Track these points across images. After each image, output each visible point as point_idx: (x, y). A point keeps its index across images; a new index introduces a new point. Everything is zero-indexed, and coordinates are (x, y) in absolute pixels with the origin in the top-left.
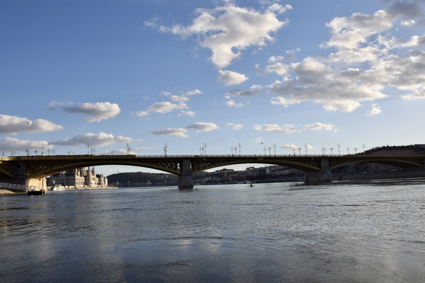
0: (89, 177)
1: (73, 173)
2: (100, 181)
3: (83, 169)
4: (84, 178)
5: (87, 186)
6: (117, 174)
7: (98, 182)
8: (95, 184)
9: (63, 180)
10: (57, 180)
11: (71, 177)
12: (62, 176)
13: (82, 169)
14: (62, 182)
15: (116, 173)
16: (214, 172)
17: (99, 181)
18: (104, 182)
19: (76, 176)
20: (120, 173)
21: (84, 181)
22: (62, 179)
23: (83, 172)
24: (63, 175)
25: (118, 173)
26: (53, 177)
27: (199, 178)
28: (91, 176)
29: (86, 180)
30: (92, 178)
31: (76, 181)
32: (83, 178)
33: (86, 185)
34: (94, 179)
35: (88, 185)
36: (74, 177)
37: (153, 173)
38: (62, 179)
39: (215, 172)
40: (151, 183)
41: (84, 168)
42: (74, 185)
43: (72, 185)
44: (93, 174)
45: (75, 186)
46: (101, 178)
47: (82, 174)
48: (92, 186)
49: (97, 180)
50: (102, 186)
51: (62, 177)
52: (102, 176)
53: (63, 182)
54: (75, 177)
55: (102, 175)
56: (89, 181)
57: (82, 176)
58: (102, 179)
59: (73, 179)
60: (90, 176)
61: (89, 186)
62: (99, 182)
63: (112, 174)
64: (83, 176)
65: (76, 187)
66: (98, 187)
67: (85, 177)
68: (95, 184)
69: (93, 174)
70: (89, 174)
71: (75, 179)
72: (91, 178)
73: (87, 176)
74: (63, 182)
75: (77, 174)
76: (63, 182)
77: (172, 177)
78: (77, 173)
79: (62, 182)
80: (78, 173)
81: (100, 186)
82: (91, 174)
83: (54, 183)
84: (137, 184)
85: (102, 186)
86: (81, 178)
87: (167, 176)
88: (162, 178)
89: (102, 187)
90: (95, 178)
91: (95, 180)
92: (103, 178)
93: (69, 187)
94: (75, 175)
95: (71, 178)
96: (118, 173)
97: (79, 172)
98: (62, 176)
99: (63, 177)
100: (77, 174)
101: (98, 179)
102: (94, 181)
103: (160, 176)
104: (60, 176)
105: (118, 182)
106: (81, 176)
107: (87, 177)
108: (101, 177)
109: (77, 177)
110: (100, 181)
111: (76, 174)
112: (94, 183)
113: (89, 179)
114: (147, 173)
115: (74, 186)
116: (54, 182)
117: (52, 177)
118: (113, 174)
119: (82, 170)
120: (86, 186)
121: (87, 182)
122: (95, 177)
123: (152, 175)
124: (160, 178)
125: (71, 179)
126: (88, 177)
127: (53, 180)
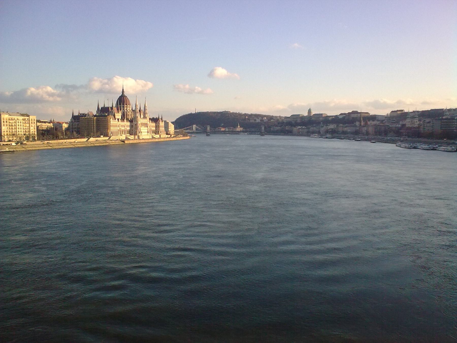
0: (136, 121)
2: (157, 127)
3: (128, 108)
4: (129, 124)
5: (133, 136)
6: (194, 114)
7: (154, 129)
8: (148, 133)
13: (125, 108)
16: (336, 116)
17: (156, 127)
18: (164, 128)
19: (111, 120)
20: (198, 112)
21: (129, 128)
25: (196, 112)
27: (314, 125)
28: (141, 121)
29: (131, 126)
31: (112, 129)
32: (127, 124)
33: (132, 135)
34: (146, 125)
35: (135, 134)
37: (245, 113)
39: (339, 115)
40: (242, 129)
41: (129, 107)
45: (110, 138)
46: (159, 123)
48: (141, 138)
49: (152, 127)
50: (160, 136)
52: (160, 120)
55: (160, 117)
56: (137, 128)
57: (125, 120)
58: (162, 124)
60: (138, 120)
61: (137, 137)
62: (156, 129)
63: (187, 114)
64: (127, 119)
67: (131, 121)
68: (148, 132)
69: (145, 117)
70: (136, 117)
72: (139, 122)
77: (272, 120)
81: (158, 136)
84: (223, 129)
85: (160, 136)
86: (122, 123)
87: (265, 118)
88: (258, 121)
90: (148, 123)
91: (147, 127)
92: (164, 122)
96: (196, 112)
97: (118, 112)
101: (154, 124)
102: (147, 128)
103: (255, 119)
105: (194, 126)
107: (133, 122)
108: (159, 121)
109: (112, 122)
110: (157, 127)
112: (147, 131)
114: (236, 113)
118: (190, 113)
120: (132, 137)
121: (133, 130)
122: (147, 121)
123: (243, 117)
124: (255, 120)
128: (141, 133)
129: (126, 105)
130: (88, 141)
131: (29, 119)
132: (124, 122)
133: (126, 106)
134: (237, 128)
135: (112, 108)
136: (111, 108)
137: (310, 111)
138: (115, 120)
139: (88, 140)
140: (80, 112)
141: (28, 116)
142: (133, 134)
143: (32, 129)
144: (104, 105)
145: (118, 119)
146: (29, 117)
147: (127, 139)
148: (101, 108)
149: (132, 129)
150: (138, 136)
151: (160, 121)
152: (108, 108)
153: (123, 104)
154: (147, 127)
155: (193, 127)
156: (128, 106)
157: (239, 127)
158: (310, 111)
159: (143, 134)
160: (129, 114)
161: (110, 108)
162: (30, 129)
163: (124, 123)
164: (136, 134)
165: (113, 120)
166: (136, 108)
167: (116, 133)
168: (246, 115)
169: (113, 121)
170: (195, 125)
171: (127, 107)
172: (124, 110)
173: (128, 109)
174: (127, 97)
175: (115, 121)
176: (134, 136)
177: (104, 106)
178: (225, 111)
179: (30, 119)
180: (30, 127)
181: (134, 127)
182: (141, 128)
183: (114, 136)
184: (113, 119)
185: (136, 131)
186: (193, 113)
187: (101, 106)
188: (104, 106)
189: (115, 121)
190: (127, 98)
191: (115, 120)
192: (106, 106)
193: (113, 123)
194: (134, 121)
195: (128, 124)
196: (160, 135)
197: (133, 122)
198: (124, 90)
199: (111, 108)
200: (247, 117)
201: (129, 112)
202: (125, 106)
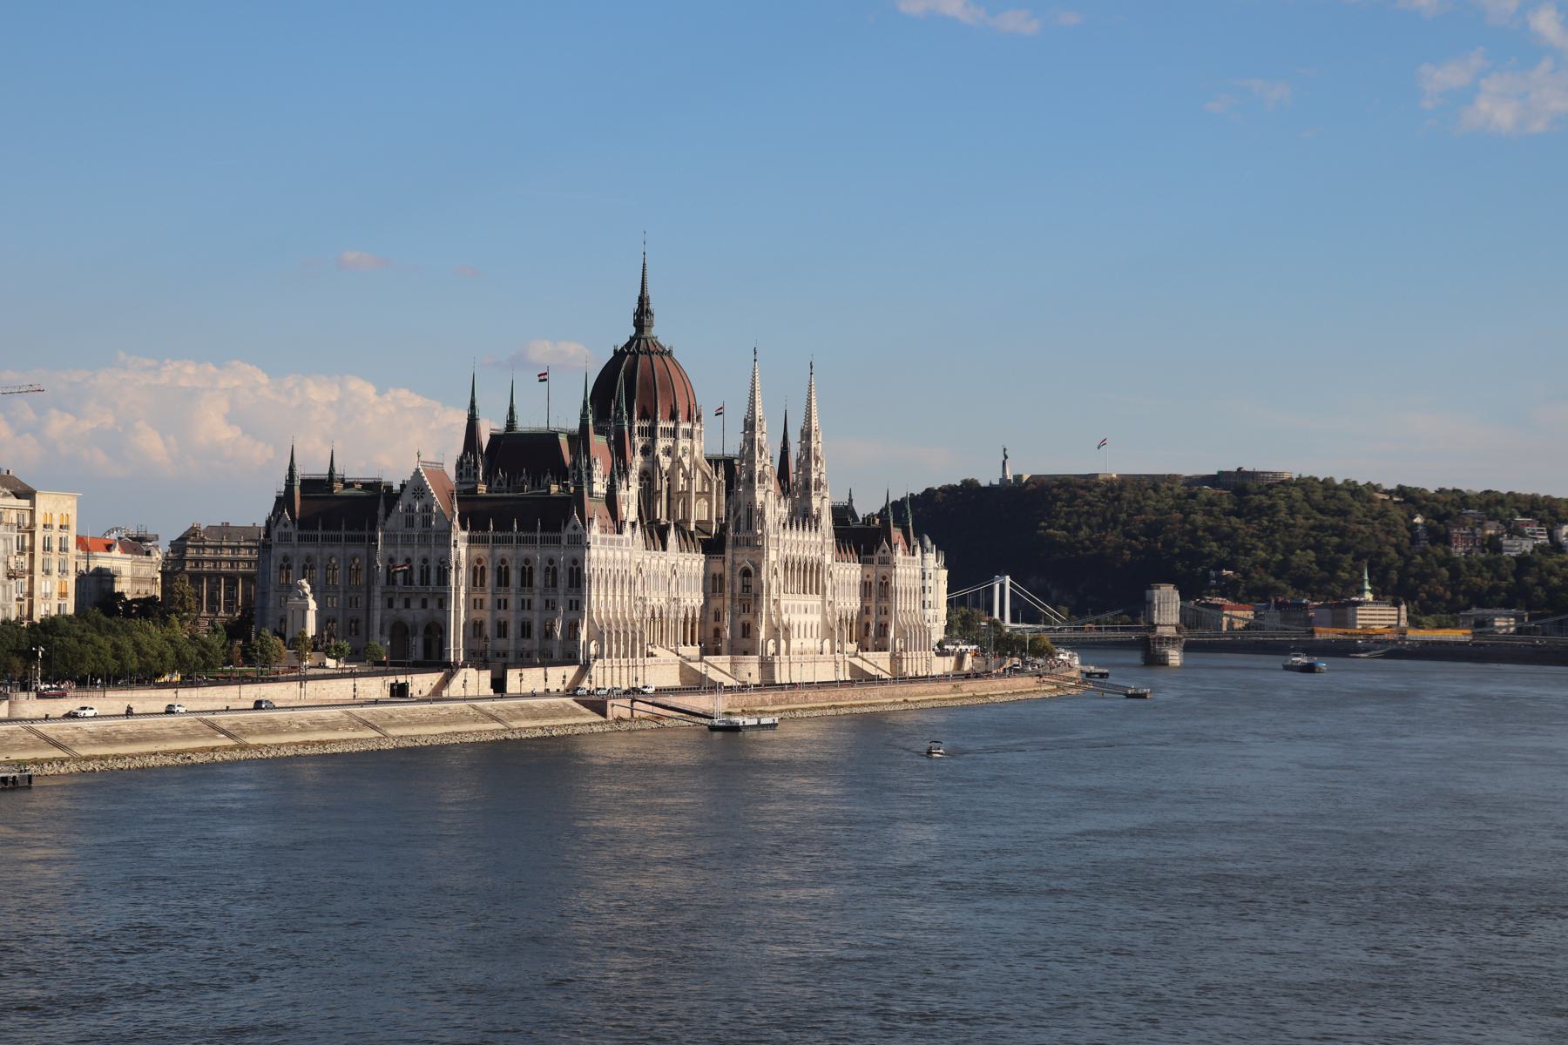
1: (554, 488)
3: (683, 443)
4: (694, 563)
6: (991, 488)
9: (425, 579)
10: (352, 572)
11: (526, 551)
12: (410, 522)
13: (662, 443)
14: (416, 605)
15: (988, 477)
19: (595, 532)
22: (417, 564)
23: (671, 476)
24: (427, 522)
26: (300, 538)
30: (789, 565)
31: (601, 602)
33: (717, 652)
34: (808, 575)
35: (744, 642)
36: (575, 553)
38: (417, 564)
42: (569, 658)
43: (547, 661)
44: (802, 516)
45: (585, 668)
47: (661, 512)
51: (408, 541)
53: (424, 605)
54: (580, 543)
57: (672, 537)
59: (551, 571)
64: (681, 527)
66: (861, 678)
67: (712, 547)
68: (828, 632)
69: (802, 516)
71: (577, 578)
72: (773, 556)
73: (723, 528)
74: (432, 604)
75: (611, 501)
76: (432, 604)
78: (600, 487)
79: (416, 605)
80: (622, 493)
81: (877, 663)
82: (770, 502)
83: (311, 629)
85: (896, 660)
89: (900, 678)
93: (499, 685)
94: (586, 522)
95: (527, 561)
96: (1004, 479)
98: (417, 531)
99: (425, 540)
100: (602, 508)
102: (814, 601)
104: (396, 521)
106: (656, 534)
111: (595, 509)
113: (746, 573)
115: (571, 671)
116: (313, 605)
117: (285, 538)
119: (668, 452)
120: (719, 668)
122: (818, 543)
125: (527, 578)
126: (736, 543)
127: (290, 588)
128: (787, 629)
129: (643, 417)
130: (445, 694)
131: (32, 513)
132: (664, 549)
133: (646, 424)
134: (1359, 603)
135: (579, 440)
136: (571, 438)
138: (616, 537)
139: (445, 682)
140: (336, 465)
141: (27, 494)
142: (724, 646)
143: (47, 596)
145: (633, 525)
146: (33, 504)
147: (696, 683)
148: (492, 436)
149: (716, 603)
150: (767, 666)
151: (900, 548)
152: (550, 438)
153: (648, 414)
154: (819, 589)
155: (991, 589)
156: (688, 426)
157: (1369, 596)
159: (795, 644)
160: (689, 492)
161: (563, 439)
162: (36, 593)
163: (662, 562)
164: (746, 643)
165: (608, 536)
166: (750, 441)
167: (633, 643)
168: (1409, 497)
169: (603, 541)
170: (1008, 579)
171: (673, 433)
172: (650, 458)
173: (659, 451)
174: (669, 353)
175: (620, 542)
176: (732, 663)
178: (1239, 469)
179: (39, 520)
180: (36, 578)
181: (728, 590)
182: (785, 601)
183: (610, 656)
184: (604, 529)
185: (746, 618)
186: (984, 483)
189: (620, 542)
190: (674, 362)
191: (620, 532)
193: (602, 554)
194: (729, 542)
195: (654, 562)
196: (893, 657)
197: (729, 552)
198: (653, 305)
199: (571, 438)
200: (1418, 520)
201: (687, 477)
202: (662, 424)
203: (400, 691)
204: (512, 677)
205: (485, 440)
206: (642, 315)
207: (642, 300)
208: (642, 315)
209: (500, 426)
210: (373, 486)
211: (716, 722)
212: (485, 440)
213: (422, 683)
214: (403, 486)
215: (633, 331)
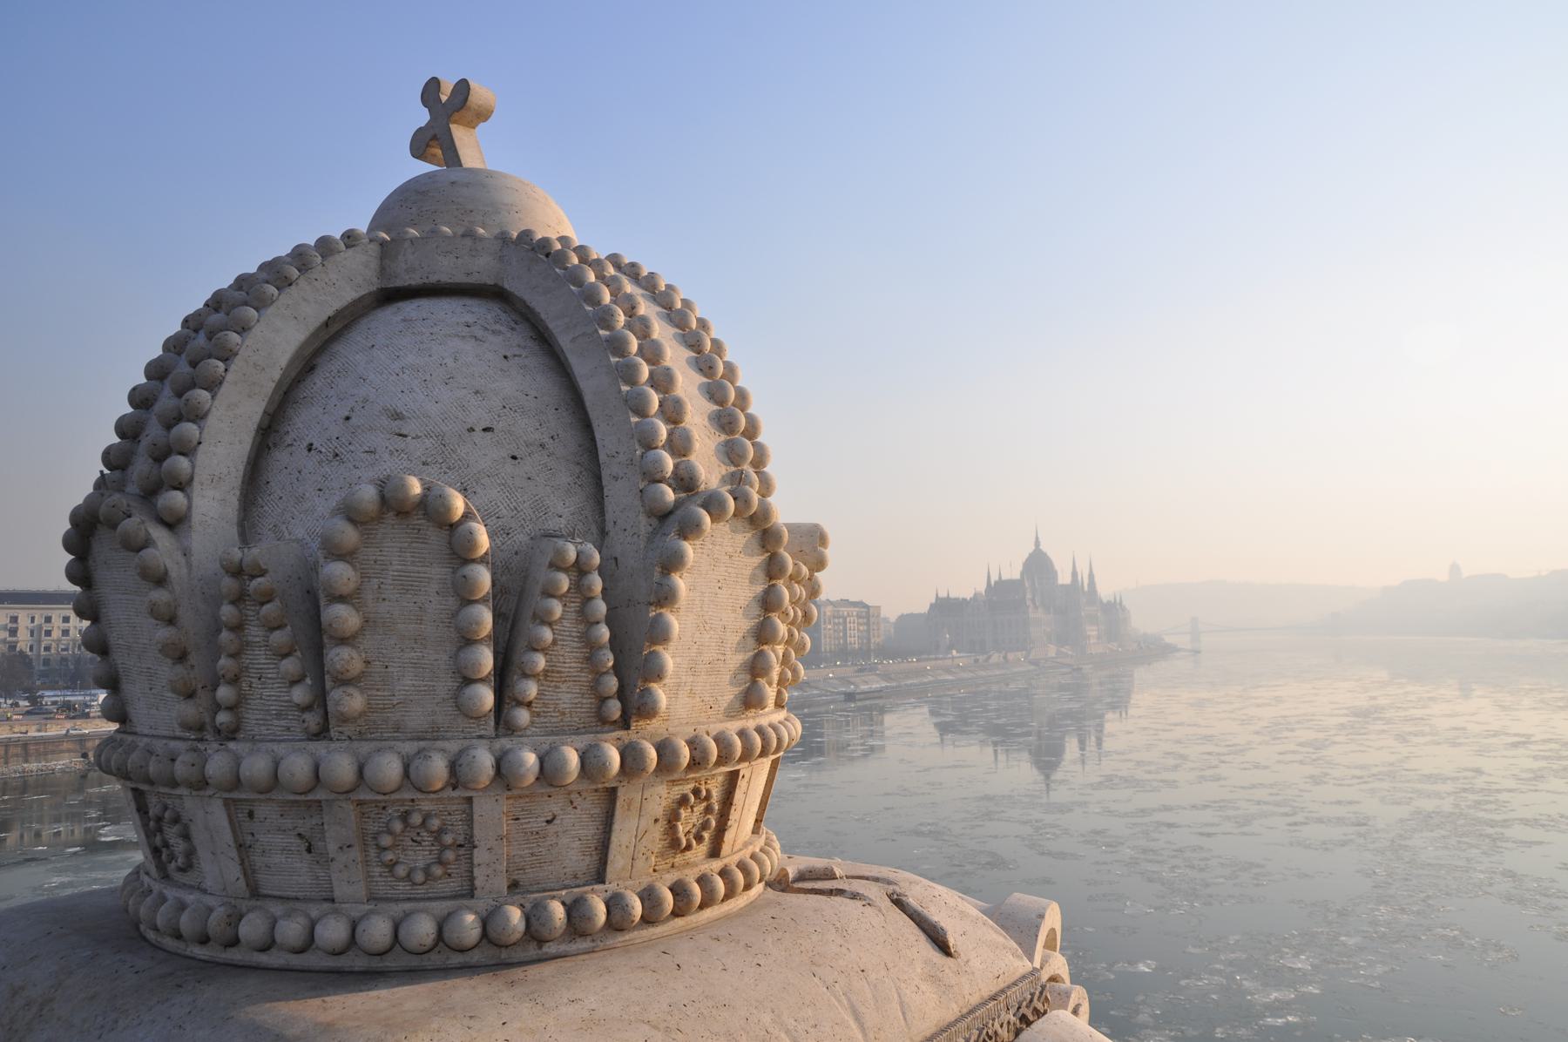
65: (1031, 657)
75: (1033, 600)
94: (1028, 607)
112: (1095, 633)
137: (1455, 569)
144: (1000, 574)
148: (996, 582)
158: (1455, 569)
177: (1000, 577)
187: (994, 578)
188: (1000, 577)
192: (1003, 578)
198: (1040, 540)
203: (976, 661)
204: (1009, 654)
205: (993, 583)
206: (1037, 543)
207: (1037, 538)
208: (1037, 543)
209: (997, 579)
210: (964, 600)
211: (1075, 667)
212: (993, 583)
213: (981, 658)
214: (971, 599)
215: (1034, 548)
